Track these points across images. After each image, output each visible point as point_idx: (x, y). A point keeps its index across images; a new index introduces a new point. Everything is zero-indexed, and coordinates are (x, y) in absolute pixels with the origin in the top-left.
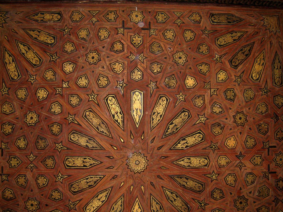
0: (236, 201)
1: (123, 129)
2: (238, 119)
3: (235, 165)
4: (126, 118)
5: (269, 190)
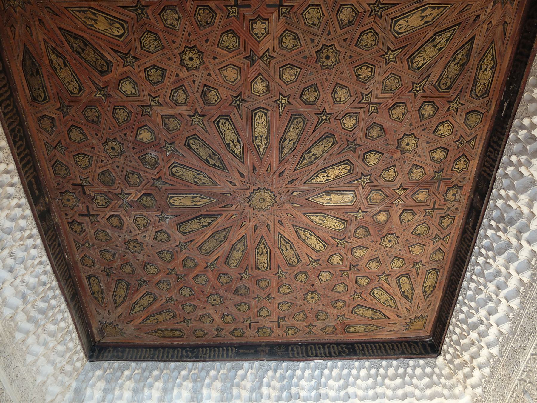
0: (324, 66)
2: (192, 62)
3: (266, 68)
5: (310, 5)
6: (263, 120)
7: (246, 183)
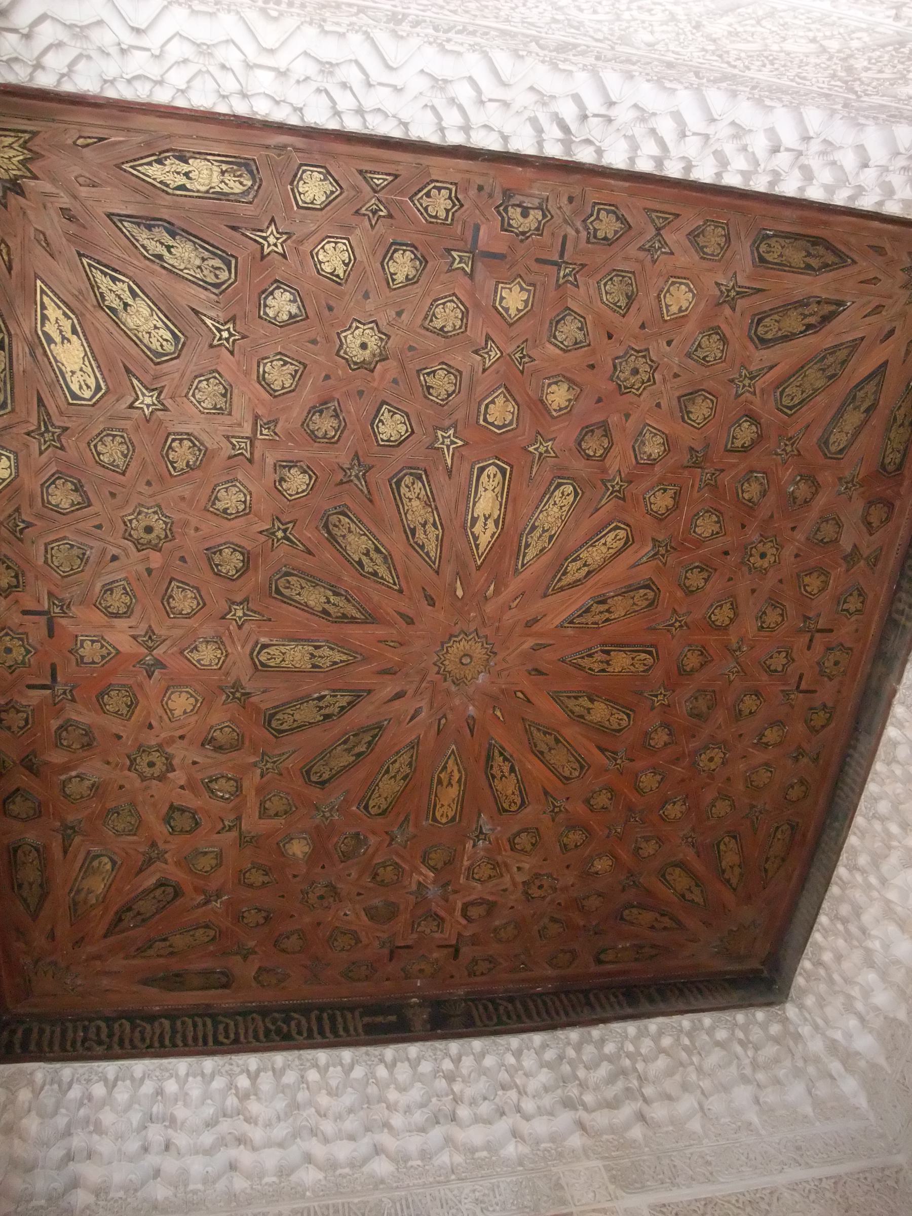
0: (166, 536)
6: (277, 653)
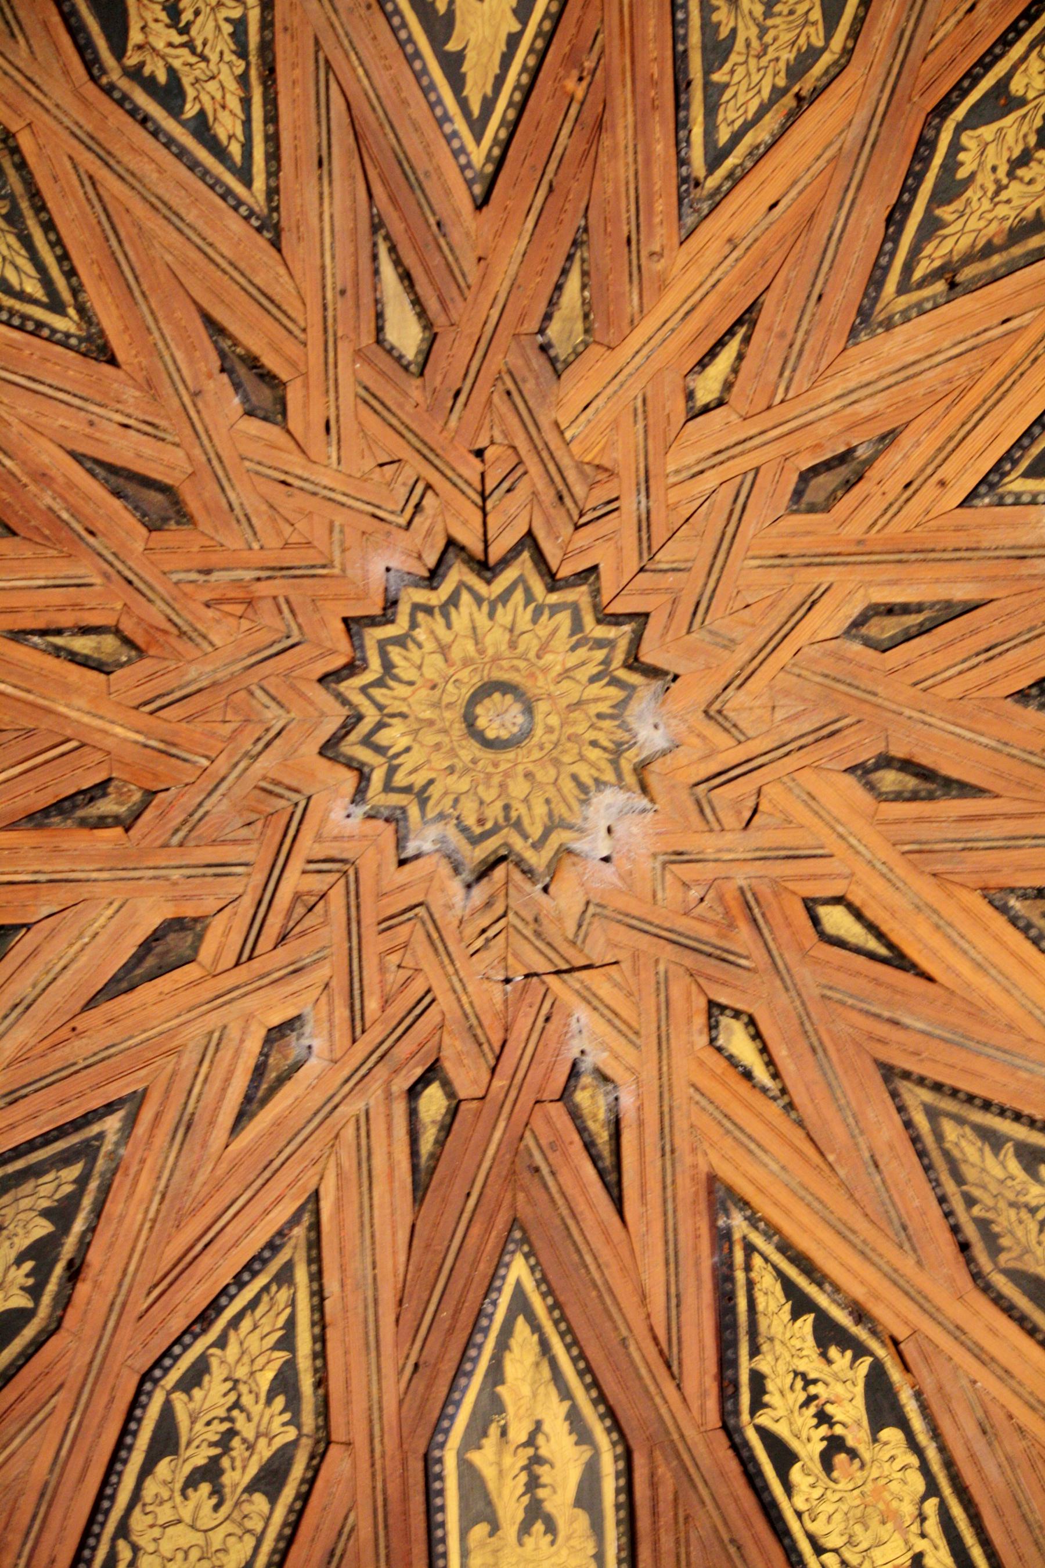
1: (738, 1224)
4: (691, 1386)
7: (264, 903)
